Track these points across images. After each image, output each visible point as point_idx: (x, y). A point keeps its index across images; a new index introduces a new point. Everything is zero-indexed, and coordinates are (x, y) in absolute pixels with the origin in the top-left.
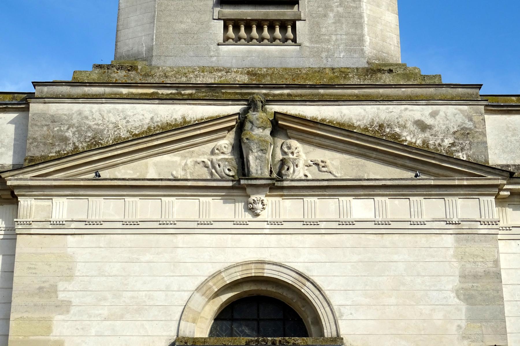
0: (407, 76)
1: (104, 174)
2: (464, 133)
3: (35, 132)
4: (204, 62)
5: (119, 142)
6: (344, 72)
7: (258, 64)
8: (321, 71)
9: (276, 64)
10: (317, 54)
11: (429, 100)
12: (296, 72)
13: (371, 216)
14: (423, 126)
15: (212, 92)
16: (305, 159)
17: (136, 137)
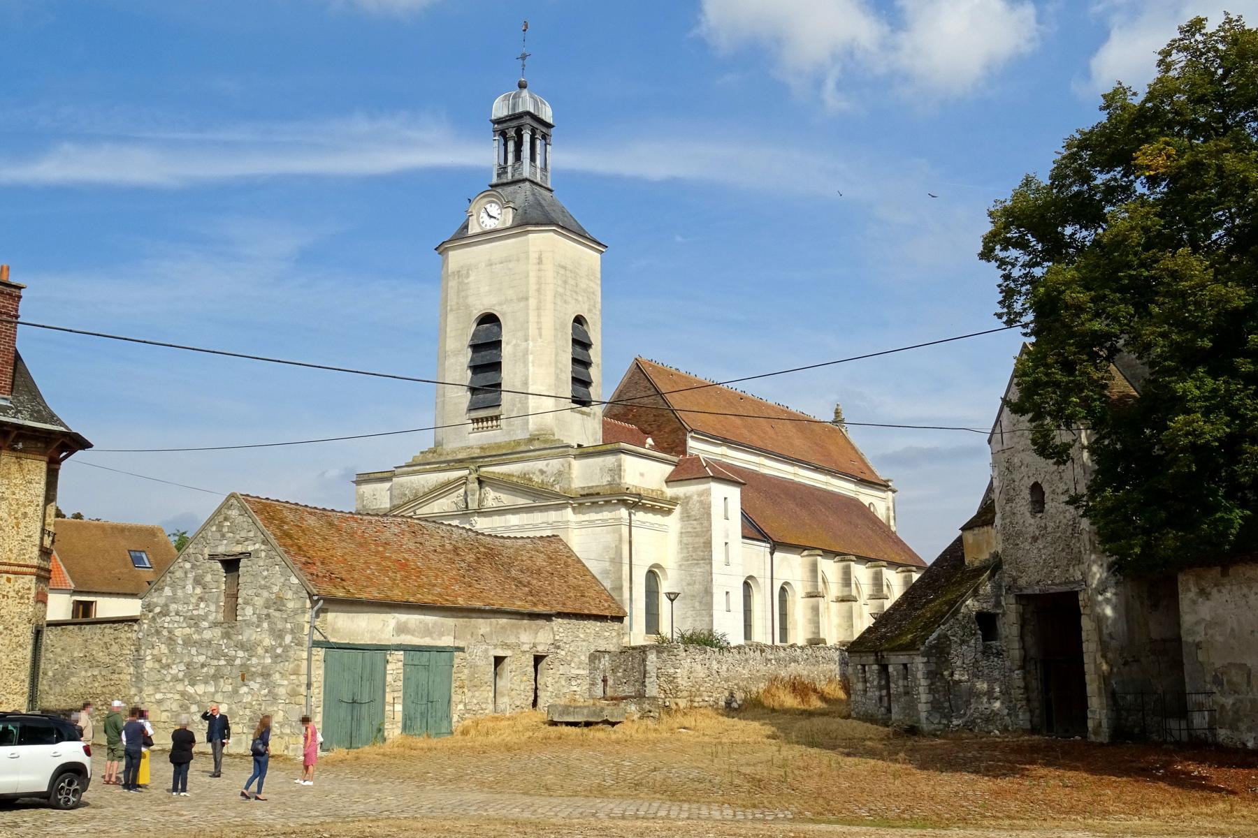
0: (546, 441)
1: (418, 512)
2: (560, 473)
3: (396, 493)
4: (463, 444)
5: (425, 494)
6: (518, 443)
7: (484, 442)
8: (508, 443)
9: (492, 441)
10: (508, 433)
11: (545, 458)
12: (499, 446)
13: (517, 523)
14: (542, 472)
15: (460, 463)
16: (492, 498)
17: (431, 492)
